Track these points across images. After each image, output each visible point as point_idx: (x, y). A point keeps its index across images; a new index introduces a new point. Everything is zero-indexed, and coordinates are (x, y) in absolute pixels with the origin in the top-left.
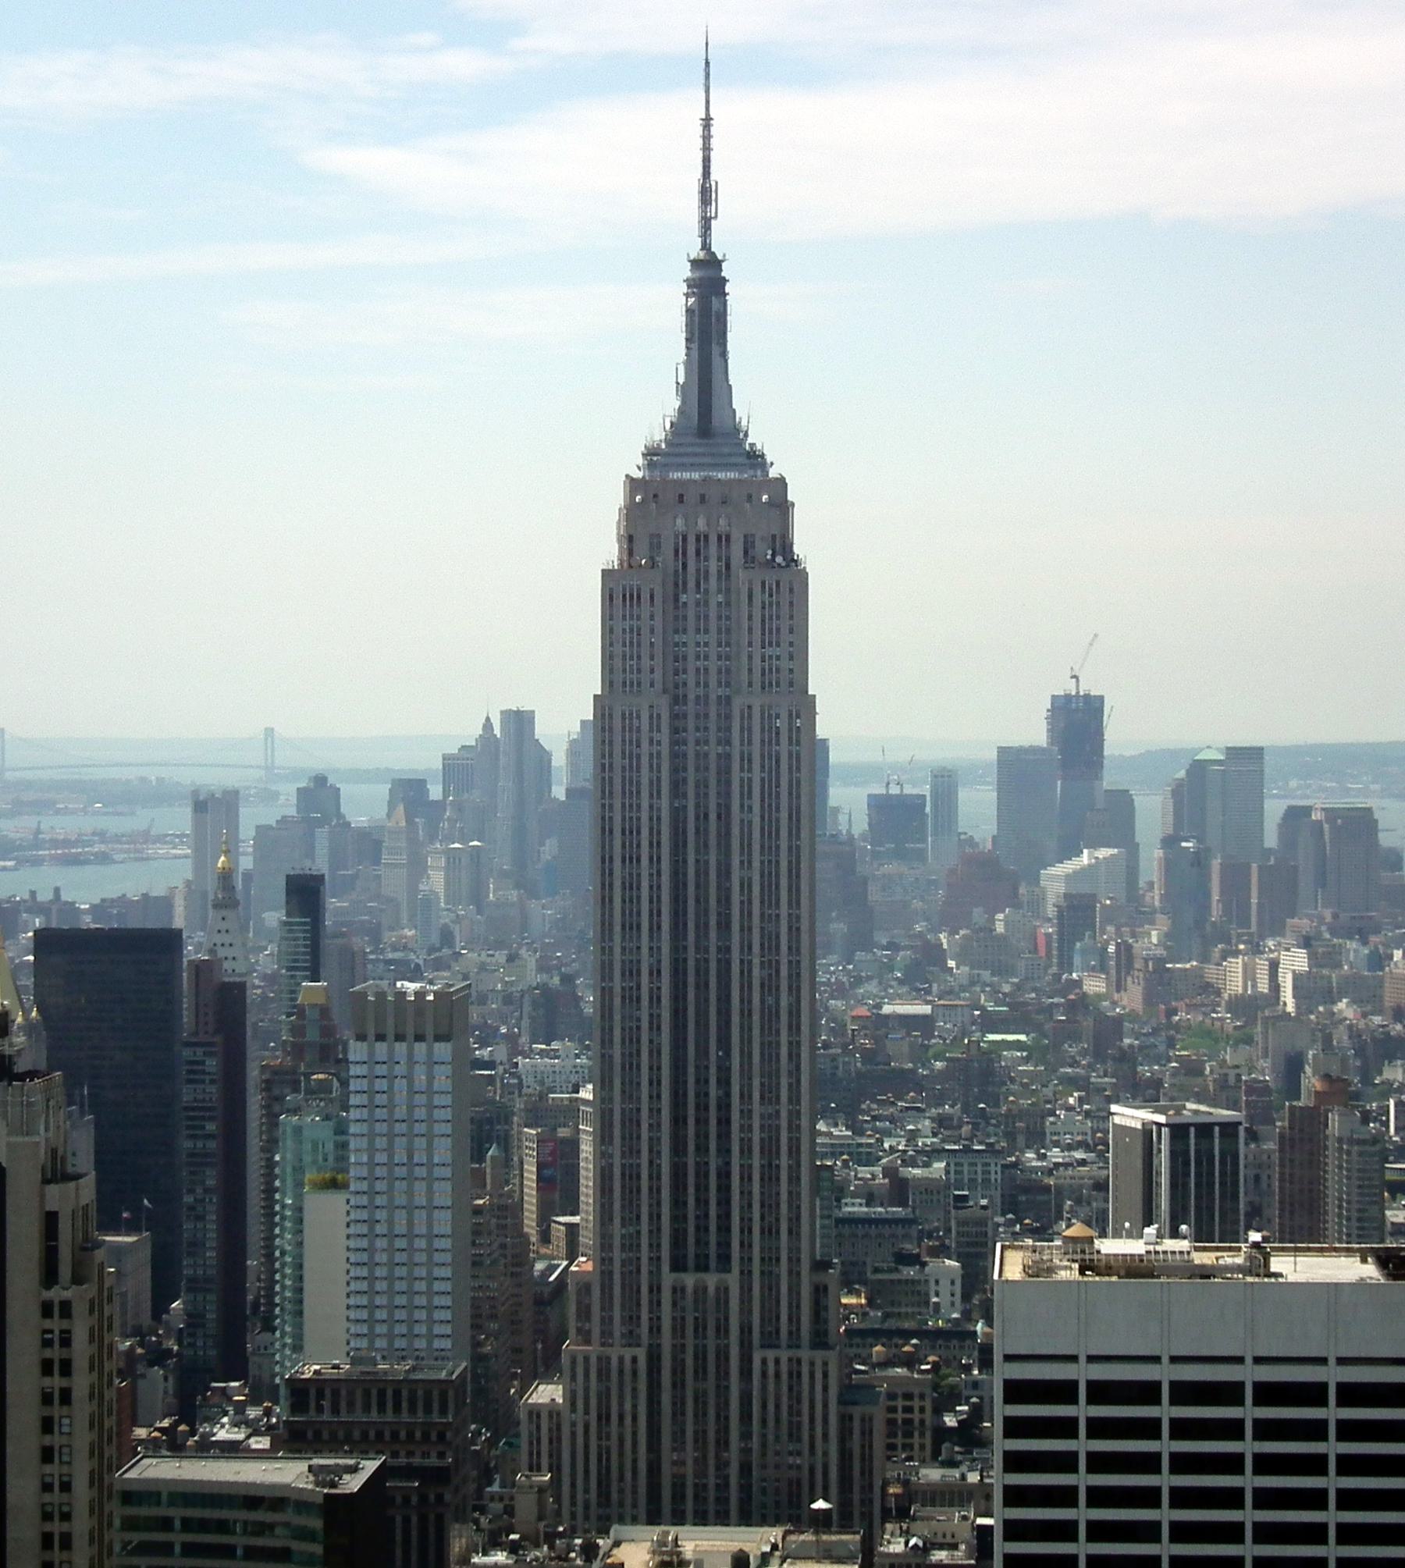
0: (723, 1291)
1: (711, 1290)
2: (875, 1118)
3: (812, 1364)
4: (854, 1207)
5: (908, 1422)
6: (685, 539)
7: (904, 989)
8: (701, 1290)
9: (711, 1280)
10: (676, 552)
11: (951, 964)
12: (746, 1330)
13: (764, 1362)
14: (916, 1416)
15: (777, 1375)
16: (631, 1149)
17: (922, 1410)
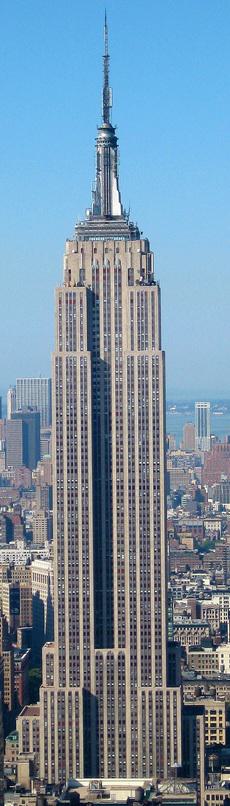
0: (122, 657)
1: (116, 657)
2: (181, 577)
3: (168, 693)
4: (178, 620)
5: (214, 725)
6: (98, 270)
7: (187, 514)
8: (110, 657)
9: (116, 651)
10: (93, 278)
11: (210, 501)
12: (134, 679)
13: (143, 693)
14: (217, 722)
15: (150, 701)
16: (74, 585)
17: (221, 719)
